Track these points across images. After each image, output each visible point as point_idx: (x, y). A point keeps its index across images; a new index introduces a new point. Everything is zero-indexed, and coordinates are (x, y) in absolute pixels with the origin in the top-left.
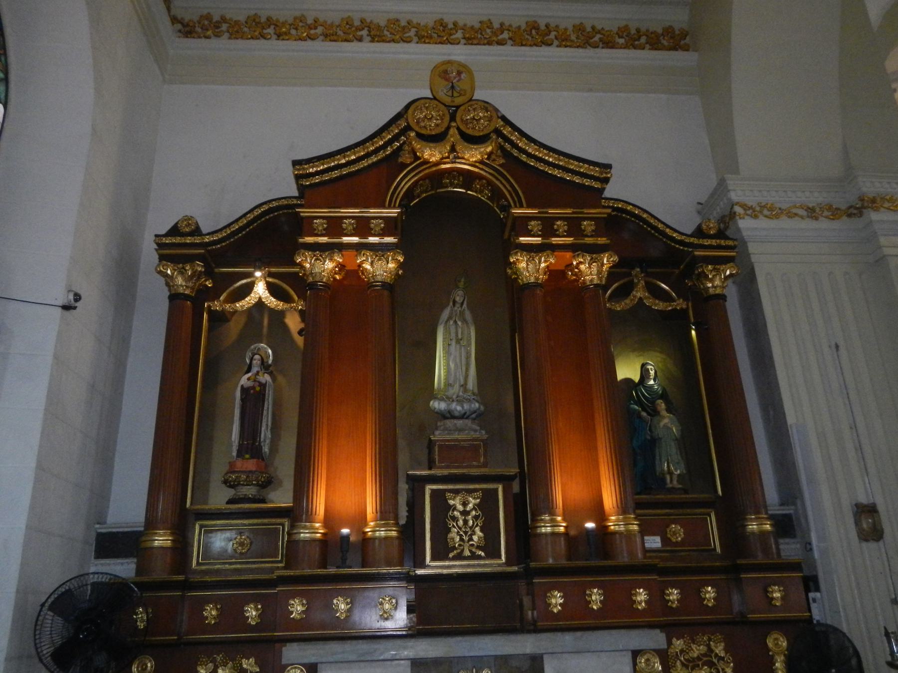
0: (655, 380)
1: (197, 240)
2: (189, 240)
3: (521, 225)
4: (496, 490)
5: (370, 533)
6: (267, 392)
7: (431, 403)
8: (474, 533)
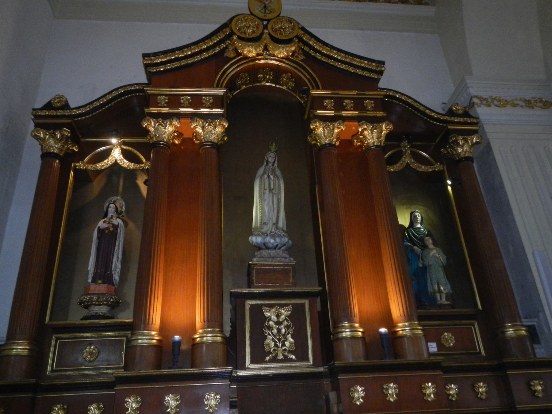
0: (421, 224)
1: (67, 113)
2: (60, 113)
3: (319, 103)
4: (304, 304)
5: (198, 339)
6: (119, 231)
7: (250, 238)
8: (286, 339)
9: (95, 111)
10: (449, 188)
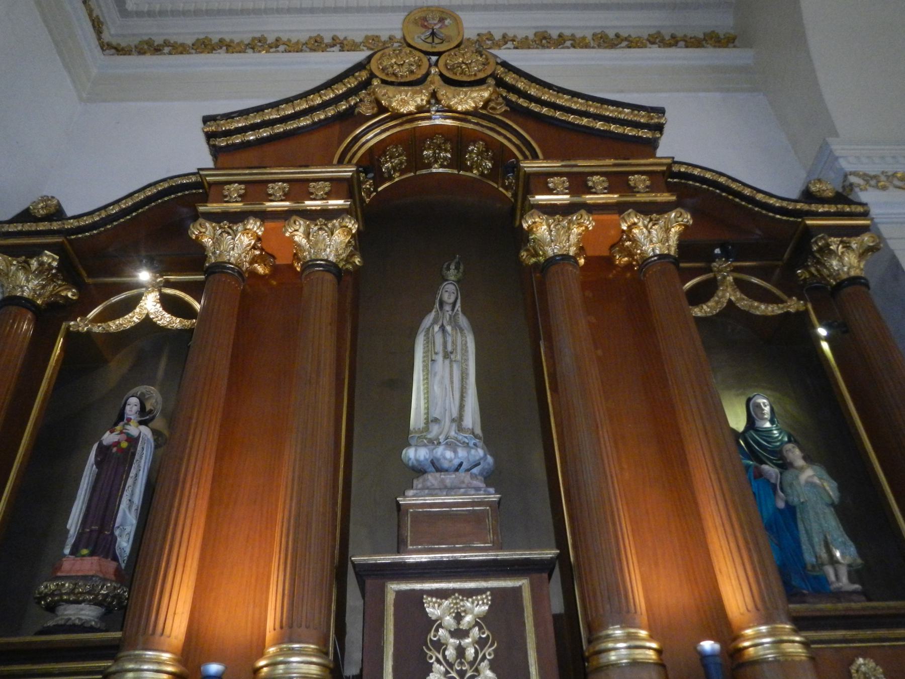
1: (55, 226)
2: (42, 226)
5: (265, 669)
6: (139, 448)
7: (404, 452)
9: (111, 222)
10: (825, 346)
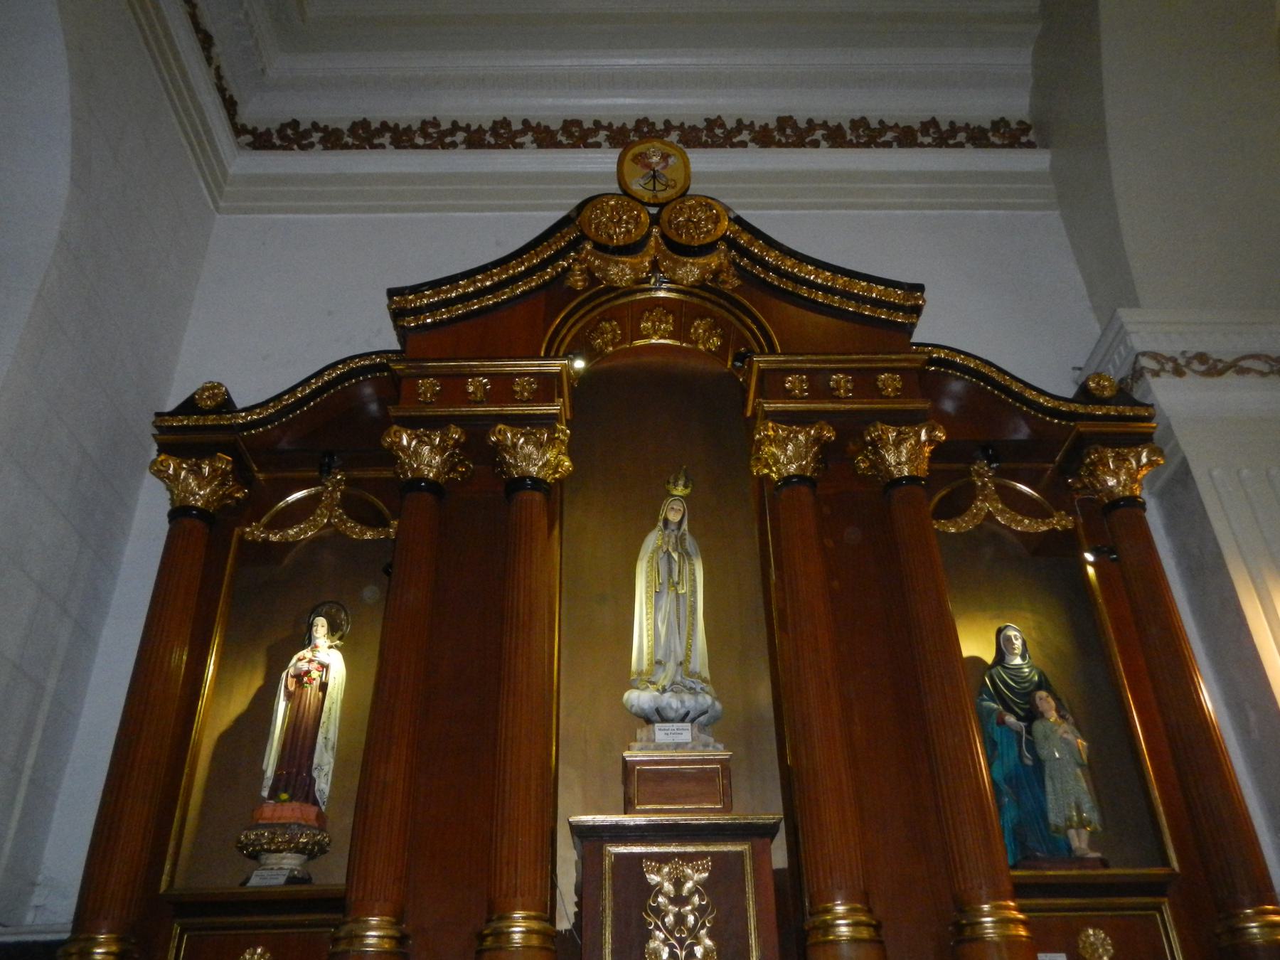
0: (1023, 657)
2: (211, 420)
8: (698, 941)
10: (1091, 571)
